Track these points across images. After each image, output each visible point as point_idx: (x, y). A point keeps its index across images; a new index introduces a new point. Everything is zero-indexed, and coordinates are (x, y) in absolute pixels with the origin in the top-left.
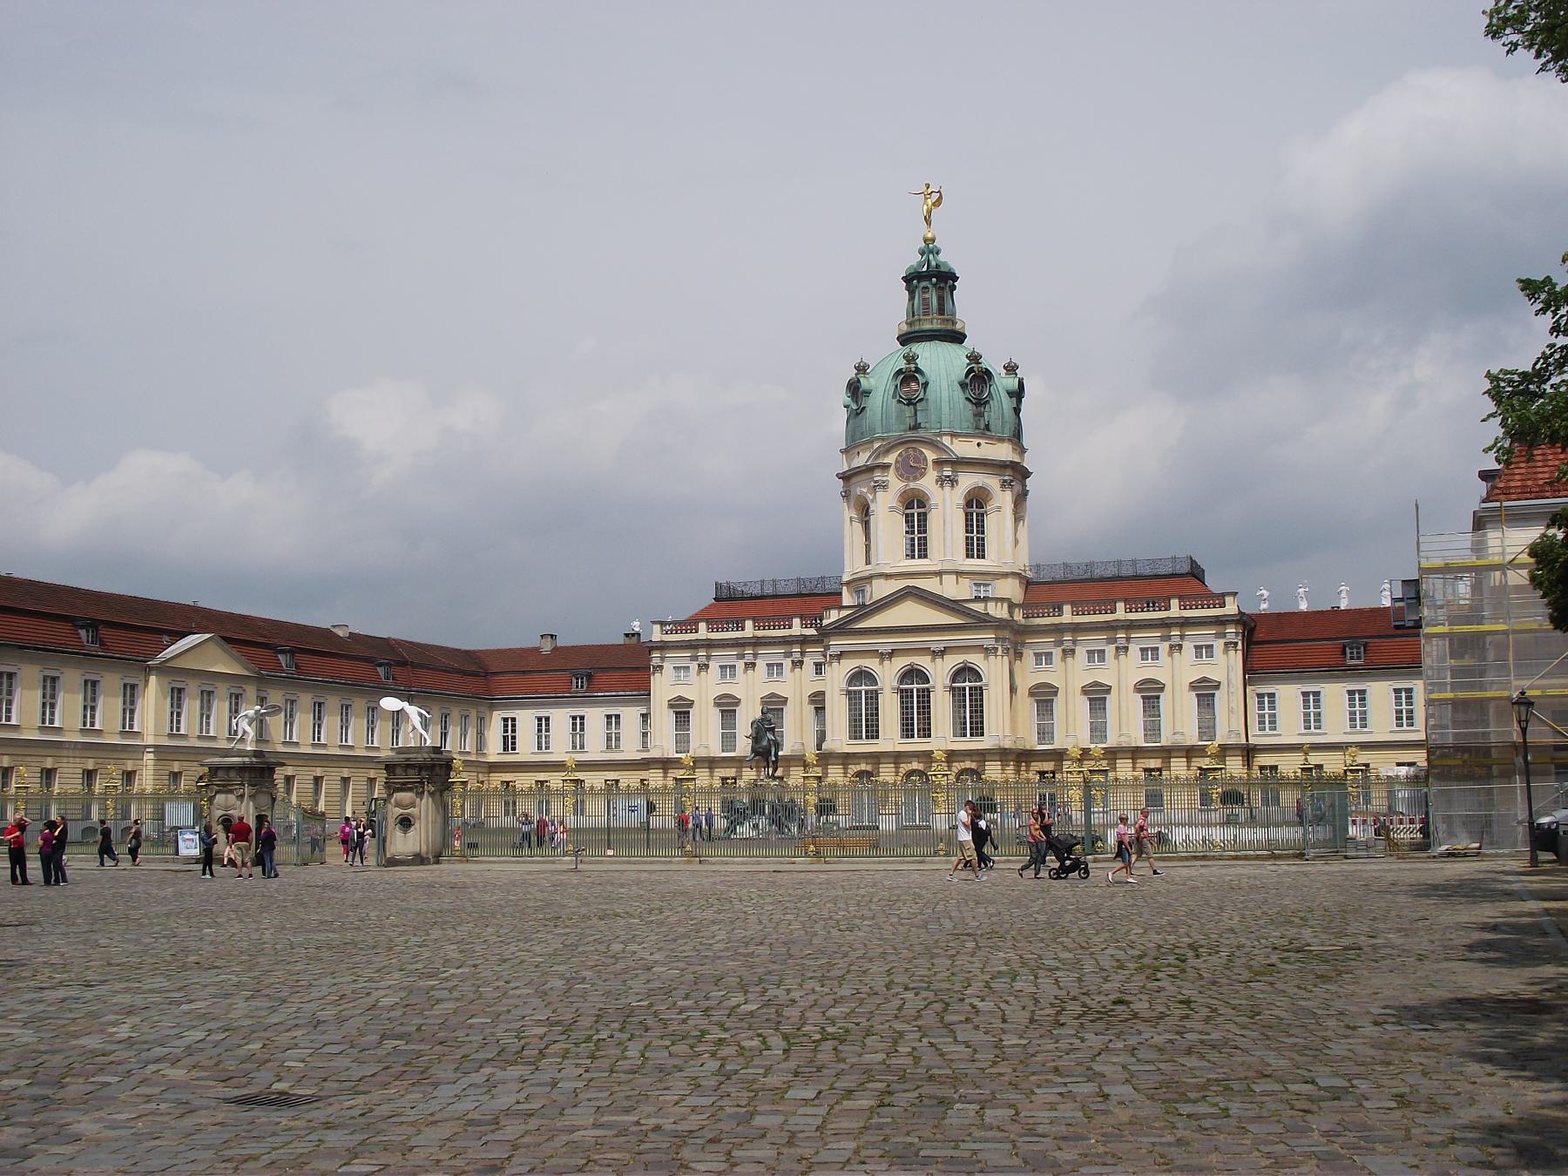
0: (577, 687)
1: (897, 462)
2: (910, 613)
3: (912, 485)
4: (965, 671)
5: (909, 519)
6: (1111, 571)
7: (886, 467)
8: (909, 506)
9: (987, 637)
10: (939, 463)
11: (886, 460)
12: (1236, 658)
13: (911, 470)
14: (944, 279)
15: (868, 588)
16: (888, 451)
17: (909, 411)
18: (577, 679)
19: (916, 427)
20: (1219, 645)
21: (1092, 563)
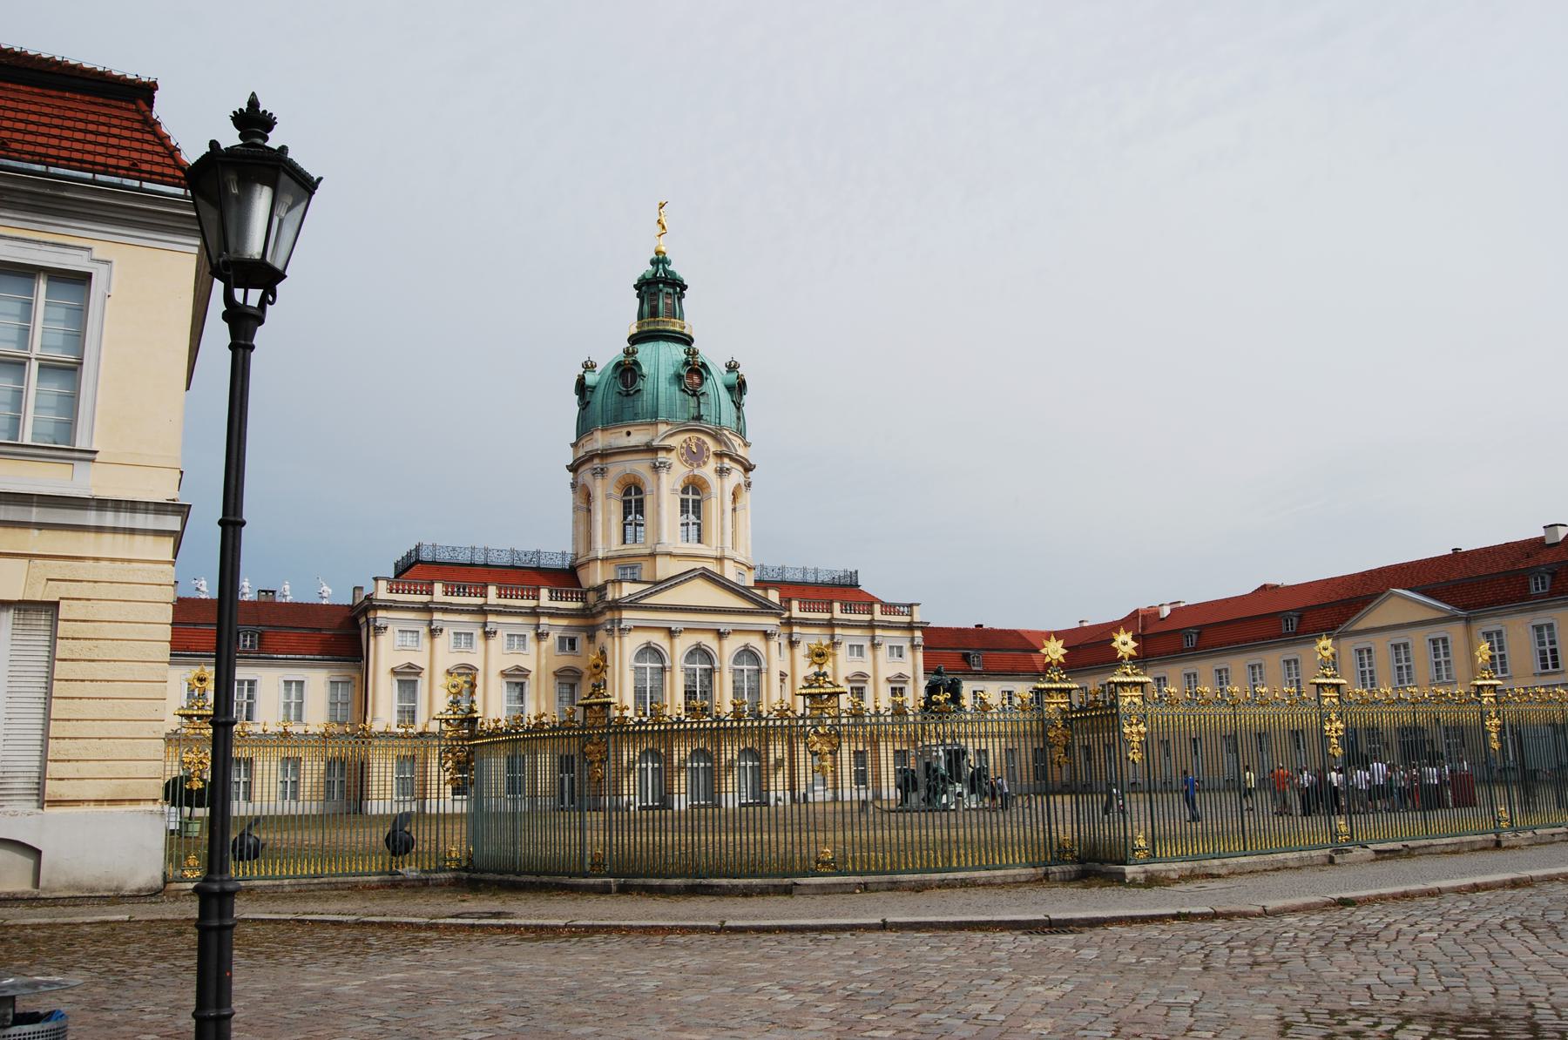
0: (245, 646)
1: (682, 447)
2: (699, 593)
3: (696, 472)
4: (748, 654)
5: (684, 503)
6: (798, 577)
7: (669, 449)
8: (685, 490)
9: (770, 623)
10: (720, 455)
11: (668, 442)
12: (920, 655)
13: (695, 456)
14: (684, 287)
15: (646, 565)
16: (671, 435)
17: (692, 402)
18: (245, 636)
19: (699, 418)
20: (906, 645)
21: (783, 568)
